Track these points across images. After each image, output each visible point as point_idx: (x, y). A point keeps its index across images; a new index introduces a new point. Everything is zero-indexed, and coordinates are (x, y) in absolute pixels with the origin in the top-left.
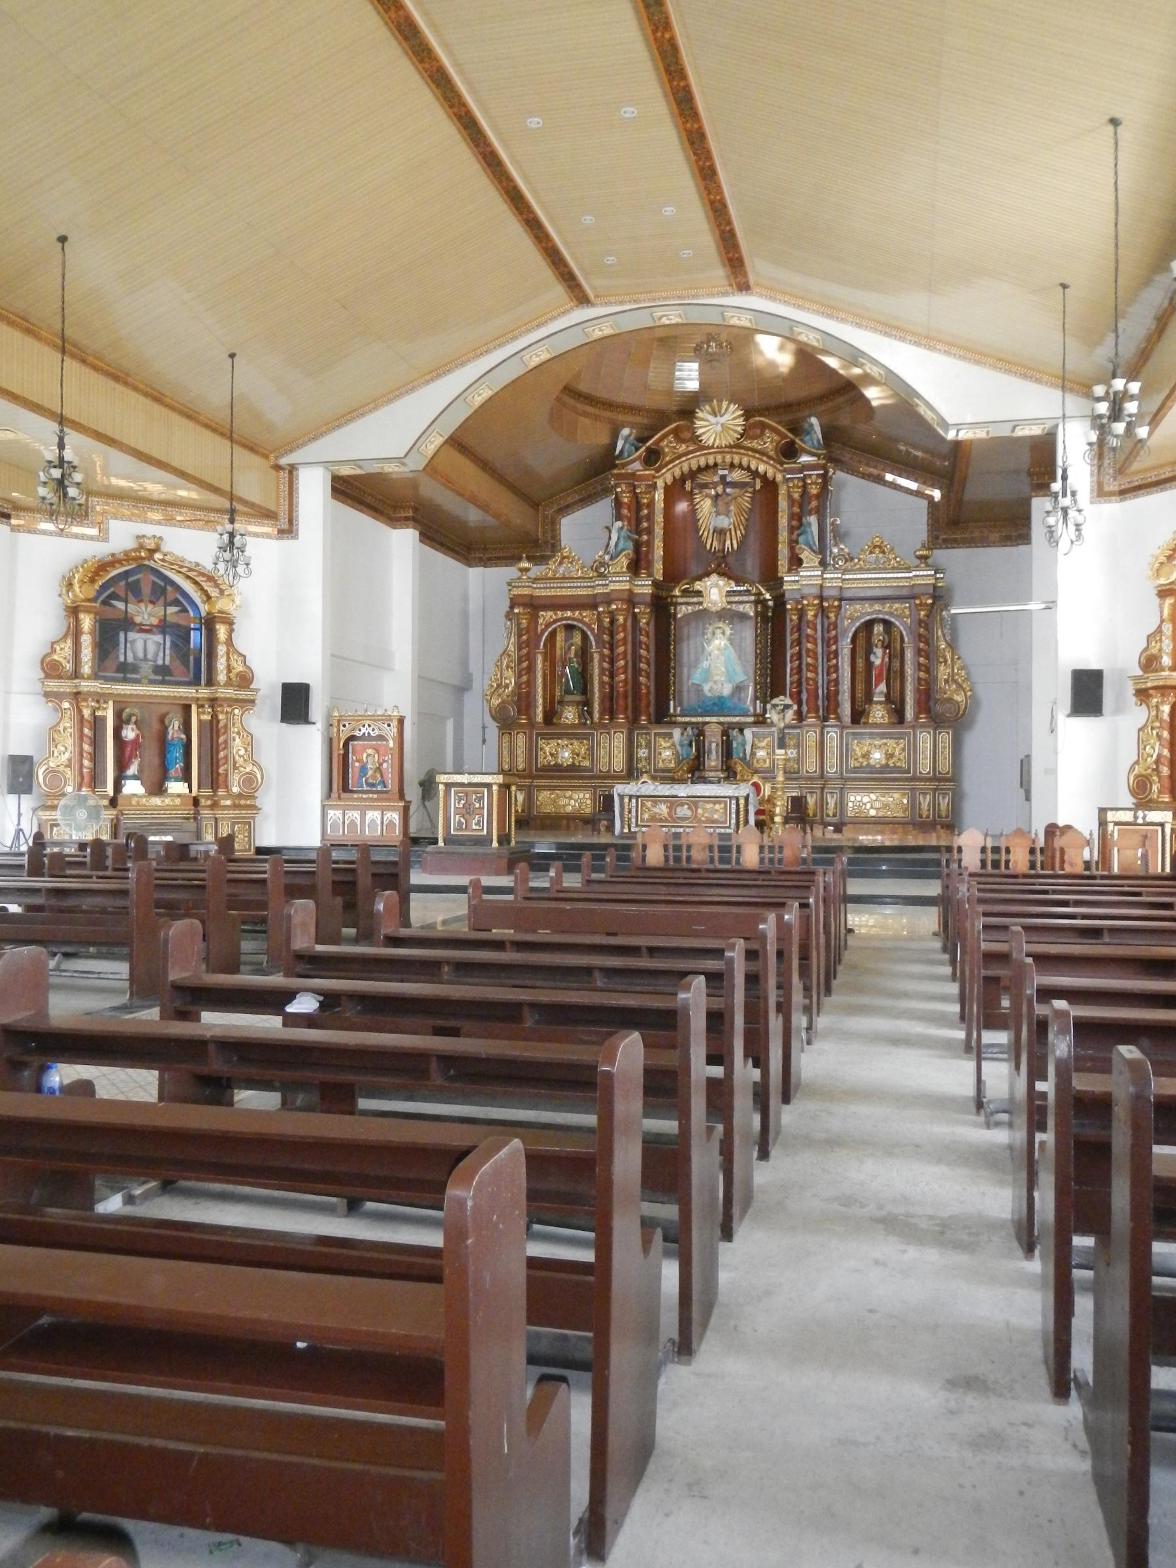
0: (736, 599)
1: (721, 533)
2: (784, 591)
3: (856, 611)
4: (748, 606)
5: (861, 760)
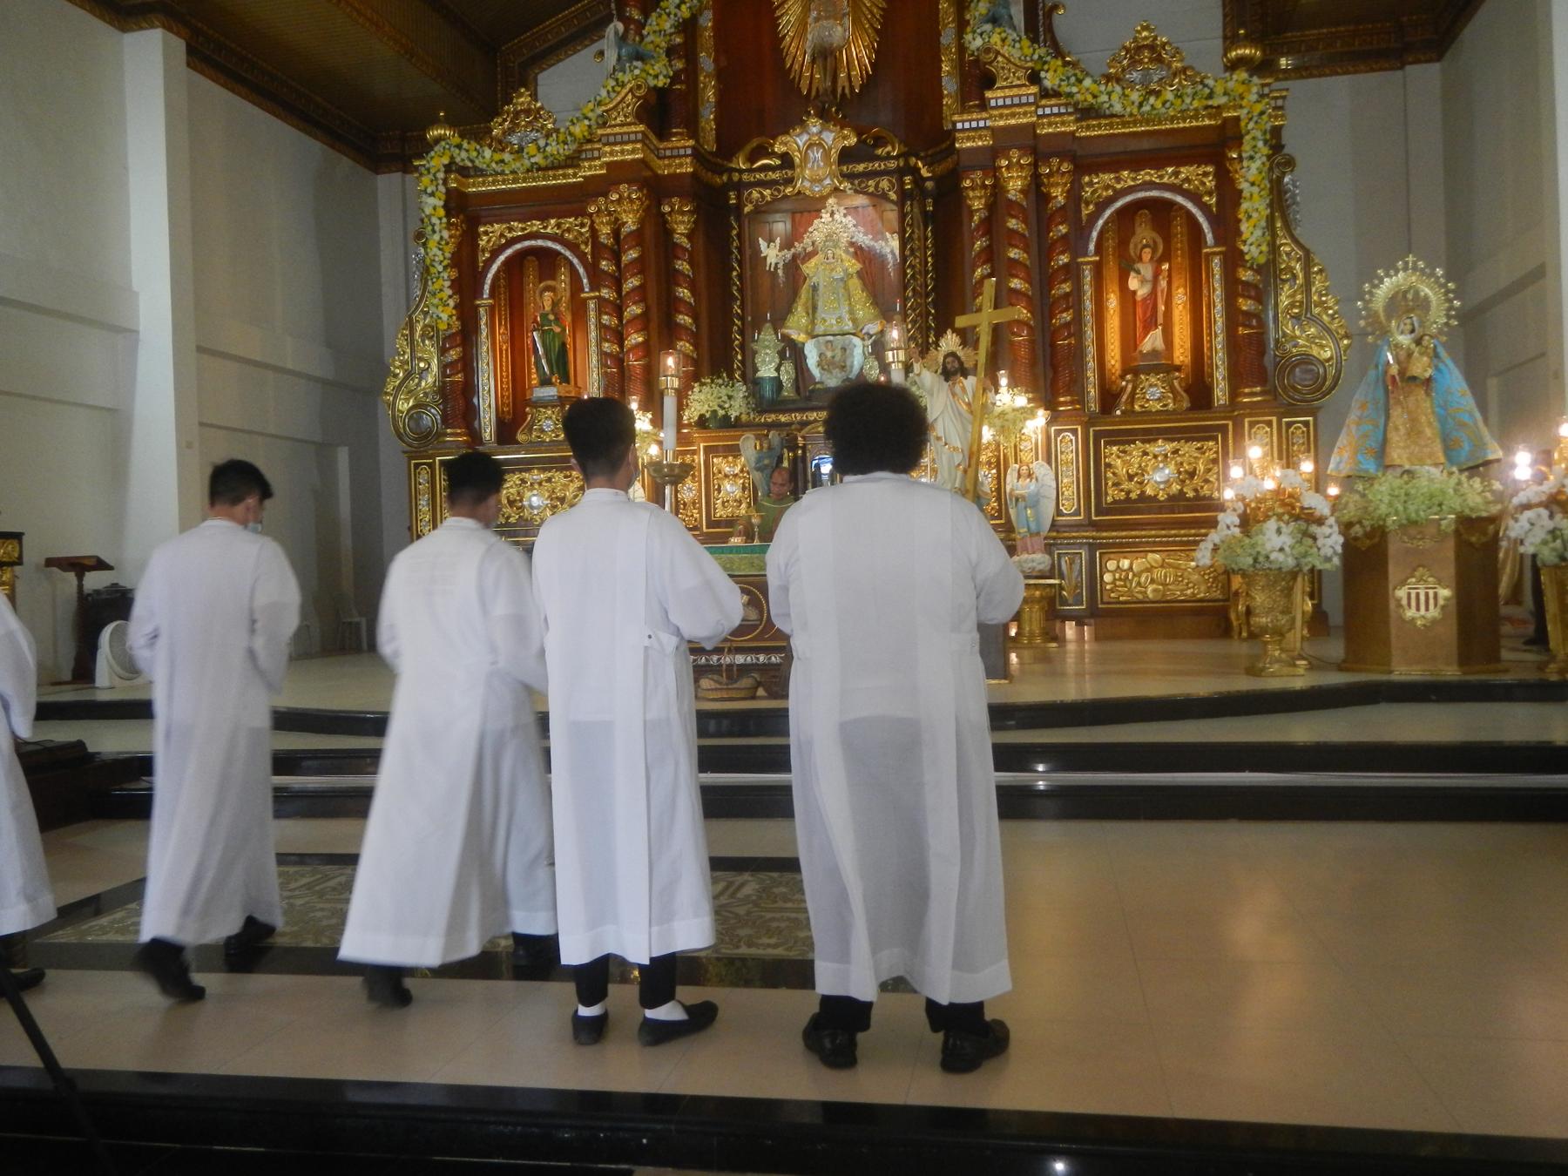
0: (861, 167)
1: (826, 55)
2: (959, 151)
3: (1107, 187)
4: (884, 184)
5: (1125, 486)
